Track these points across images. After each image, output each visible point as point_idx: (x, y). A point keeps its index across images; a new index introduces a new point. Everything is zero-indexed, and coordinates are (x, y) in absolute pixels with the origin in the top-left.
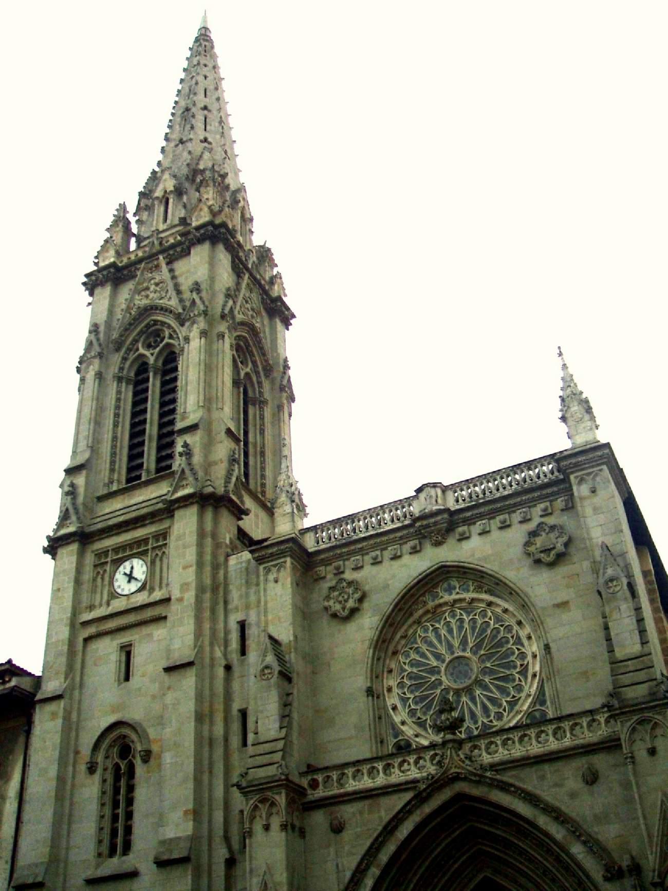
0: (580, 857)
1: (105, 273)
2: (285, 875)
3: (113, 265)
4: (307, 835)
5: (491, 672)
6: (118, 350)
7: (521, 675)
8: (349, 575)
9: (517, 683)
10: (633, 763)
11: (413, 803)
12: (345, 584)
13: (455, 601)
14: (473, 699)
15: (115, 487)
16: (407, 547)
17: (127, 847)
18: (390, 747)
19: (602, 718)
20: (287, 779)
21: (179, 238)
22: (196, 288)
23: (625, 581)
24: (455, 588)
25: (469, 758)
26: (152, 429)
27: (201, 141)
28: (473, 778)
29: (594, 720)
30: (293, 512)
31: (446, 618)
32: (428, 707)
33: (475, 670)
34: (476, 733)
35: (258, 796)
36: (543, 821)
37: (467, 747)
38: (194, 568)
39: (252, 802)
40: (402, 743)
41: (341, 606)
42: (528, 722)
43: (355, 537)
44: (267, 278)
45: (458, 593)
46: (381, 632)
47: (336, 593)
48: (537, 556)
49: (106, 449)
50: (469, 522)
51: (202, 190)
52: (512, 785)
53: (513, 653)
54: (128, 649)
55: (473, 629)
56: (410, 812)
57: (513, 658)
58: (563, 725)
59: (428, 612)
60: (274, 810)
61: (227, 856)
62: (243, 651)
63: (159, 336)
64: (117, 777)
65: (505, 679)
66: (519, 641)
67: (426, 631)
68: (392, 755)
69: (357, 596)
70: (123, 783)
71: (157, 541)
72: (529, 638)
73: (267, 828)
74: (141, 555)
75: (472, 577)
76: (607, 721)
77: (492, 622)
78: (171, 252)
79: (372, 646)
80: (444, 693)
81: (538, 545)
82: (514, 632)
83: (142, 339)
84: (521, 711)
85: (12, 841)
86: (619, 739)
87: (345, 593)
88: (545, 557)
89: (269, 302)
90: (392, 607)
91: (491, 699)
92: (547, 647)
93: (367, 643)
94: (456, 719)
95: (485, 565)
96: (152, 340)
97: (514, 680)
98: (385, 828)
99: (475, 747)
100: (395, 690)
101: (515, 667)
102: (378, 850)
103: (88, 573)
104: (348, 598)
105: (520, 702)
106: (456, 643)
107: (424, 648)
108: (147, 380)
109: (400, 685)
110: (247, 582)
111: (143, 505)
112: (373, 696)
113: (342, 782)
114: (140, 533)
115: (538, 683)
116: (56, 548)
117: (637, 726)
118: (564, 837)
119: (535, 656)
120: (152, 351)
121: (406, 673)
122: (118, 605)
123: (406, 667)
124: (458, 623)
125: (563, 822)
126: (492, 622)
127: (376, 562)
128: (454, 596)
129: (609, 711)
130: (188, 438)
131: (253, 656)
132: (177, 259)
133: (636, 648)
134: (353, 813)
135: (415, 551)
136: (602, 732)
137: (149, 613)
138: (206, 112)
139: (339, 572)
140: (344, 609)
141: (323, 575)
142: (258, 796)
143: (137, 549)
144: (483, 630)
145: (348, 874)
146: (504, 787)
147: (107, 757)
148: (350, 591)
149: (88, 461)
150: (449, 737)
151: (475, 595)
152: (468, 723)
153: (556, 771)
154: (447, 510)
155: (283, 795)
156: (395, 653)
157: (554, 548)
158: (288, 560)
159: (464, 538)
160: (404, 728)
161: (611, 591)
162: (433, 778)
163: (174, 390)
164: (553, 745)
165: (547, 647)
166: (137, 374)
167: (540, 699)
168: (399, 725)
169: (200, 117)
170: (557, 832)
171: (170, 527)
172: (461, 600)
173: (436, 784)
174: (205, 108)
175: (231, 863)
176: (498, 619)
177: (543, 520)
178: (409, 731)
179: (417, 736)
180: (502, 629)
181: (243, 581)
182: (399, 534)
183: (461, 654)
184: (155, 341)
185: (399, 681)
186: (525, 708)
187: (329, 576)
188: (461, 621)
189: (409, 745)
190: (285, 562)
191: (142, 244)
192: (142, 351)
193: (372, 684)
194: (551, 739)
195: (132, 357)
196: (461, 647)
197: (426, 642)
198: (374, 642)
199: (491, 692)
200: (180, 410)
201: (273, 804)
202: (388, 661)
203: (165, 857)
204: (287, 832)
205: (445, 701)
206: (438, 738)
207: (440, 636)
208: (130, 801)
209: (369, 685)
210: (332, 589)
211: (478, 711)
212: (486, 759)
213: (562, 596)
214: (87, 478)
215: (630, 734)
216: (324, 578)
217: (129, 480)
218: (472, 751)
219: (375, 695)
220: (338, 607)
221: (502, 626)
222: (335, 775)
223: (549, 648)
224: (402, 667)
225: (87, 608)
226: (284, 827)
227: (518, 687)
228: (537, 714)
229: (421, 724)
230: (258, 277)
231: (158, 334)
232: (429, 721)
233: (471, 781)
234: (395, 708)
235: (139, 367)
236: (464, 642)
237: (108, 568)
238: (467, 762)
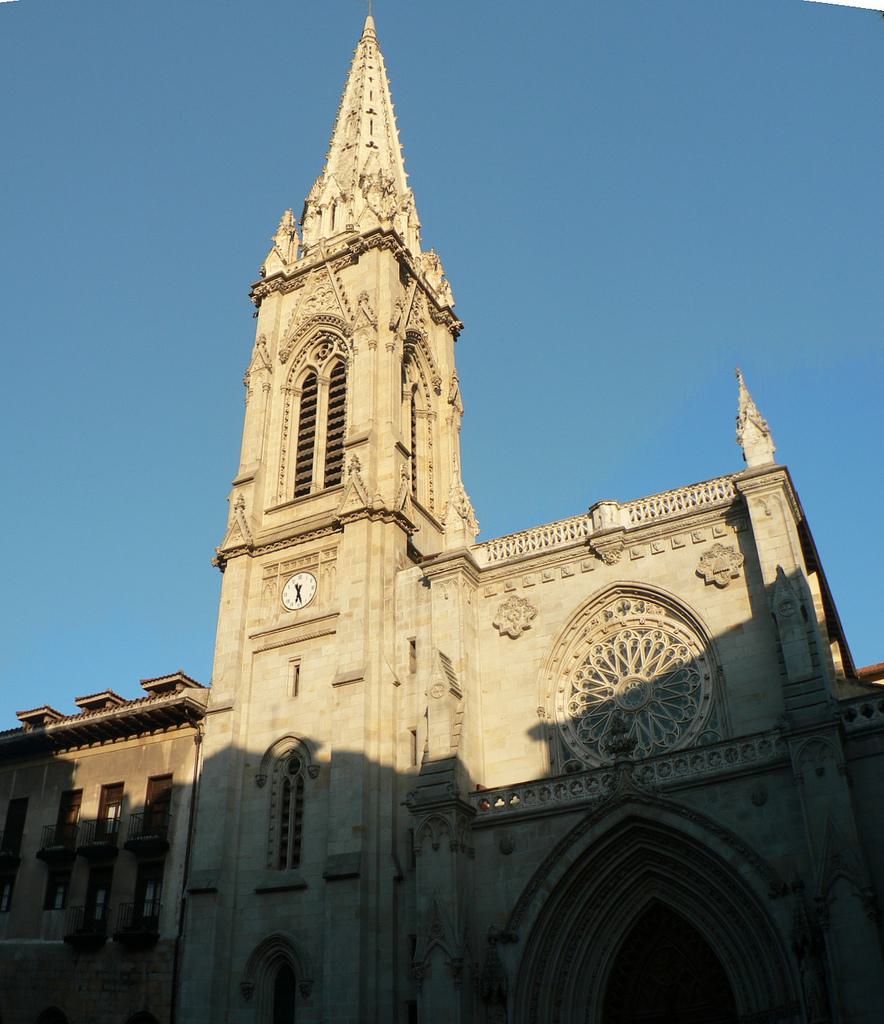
1: (272, 282)
3: (281, 275)
6: (283, 363)
8: (521, 593)
10: (803, 783)
12: (516, 602)
14: (645, 721)
15: (283, 501)
17: (296, 859)
18: (561, 769)
19: (773, 739)
20: (458, 799)
21: (347, 246)
22: (364, 298)
23: (799, 604)
24: (629, 608)
25: (641, 780)
26: (321, 442)
27: (367, 146)
28: (644, 800)
30: (464, 529)
32: (600, 730)
34: (647, 755)
36: (712, 842)
37: (639, 769)
38: (364, 583)
39: (422, 820)
40: (573, 765)
42: (699, 744)
43: (528, 555)
44: (435, 288)
49: (273, 462)
50: (642, 540)
51: (369, 196)
52: (682, 807)
53: (686, 675)
54: (296, 663)
56: (580, 834)
57: (685, 680)
58: (734, 747)
61: (396, 874)
62: (413, 671)
63: (326, 347)
64: (287, 791)
65: (678, 700)
67: (599, 651)
68: (563, 777)
69: (529, 614)
70: (292, 797)
71: (327, 554)
73: (436, 847)
74: (309, 569)
76: (777, 744)
78: (339, 261)
80: (616, 714)
83: (309, 351)
84: (692, 734)
85: (185, 846)
86: (790, 760)
89: (436, 310)
91: (663, 721)
92: (720, 669)
94: (629, 741)
96: (319, 349)
97: (686, 702)
98: (556, 849)
99: (647, 768)
103: (257, 585)
105: (692, 724)
107: (598, 668)
108: (315, 392)
110: (417, 598)
111: (313, 519)
114: (309, 547)
116: (226, 561)
119: (707, 679)
120: (319, 362)
122: (287, 619)
123: (579, 688)
124: (632, 644)
125: (732, 842)
127: (548, 580)
129: (782, 733)
130: (357, 451)
131: (423, 673)
132: (343, 268)
133: (809, 670)
135: (587, 570)
136: (774, 752)
137: (316, 628)
138: (372, 115)
139: (510, 590)
143: (308, 563)
144: (657, 652)
146: (675, 809)
147: (276, 771)
149: (257, 471)
150: (621, 758)
152: (640, 745)
154: (623, 530)
155: (454, 814)
158: (460, 575)
159: (636, 557)
160: (575, 749)
161: (785, 614)
162: (604, 800)
163: (342, 402)
164: (725, 766)
165: (720, 669)
166: (304, 386)
167: (712, 721)
168: (571, 747)
169: (366, 118)
170: (727, 853)
171: (339, 542)
173: (607, 806)
174: (371, 111)
175: (399, 879)
176: (673, 640)
177: (718, 541)
178: (579, 752)
179: (587, 758)
181: (414, 597)
182: (573, 551)
184: (324, 352)
186: (696, 730)
187: (499, 594)
188: (636, 642)
189: (579, 767)
190: (457, 578)
191: (309, 253)
192: (311, 362)
194: (724, 761)
195: (299, 368)
199: (664, 714)
200: (348, 424)
201: (444, 823)
203: (335, 872)
205: (617, 721)
206: (610, 760)
207: (613, 656)
208: (299, 815)
210: (505, 606)
211: (650, 733)
212: (658, 781)
214: (256, 491)
217: (297, 494)
218: (645, 773)
224: (574, 688)
225: (256, 621)
227: (690, 709)
228: (709, 736)
229: (593, 746)
230: (425, 285)
231: (326, 344)
232: (600, 743)
233: (644, 803)
235: (308, 378)
237: (279, 581)
238: (640, 784)
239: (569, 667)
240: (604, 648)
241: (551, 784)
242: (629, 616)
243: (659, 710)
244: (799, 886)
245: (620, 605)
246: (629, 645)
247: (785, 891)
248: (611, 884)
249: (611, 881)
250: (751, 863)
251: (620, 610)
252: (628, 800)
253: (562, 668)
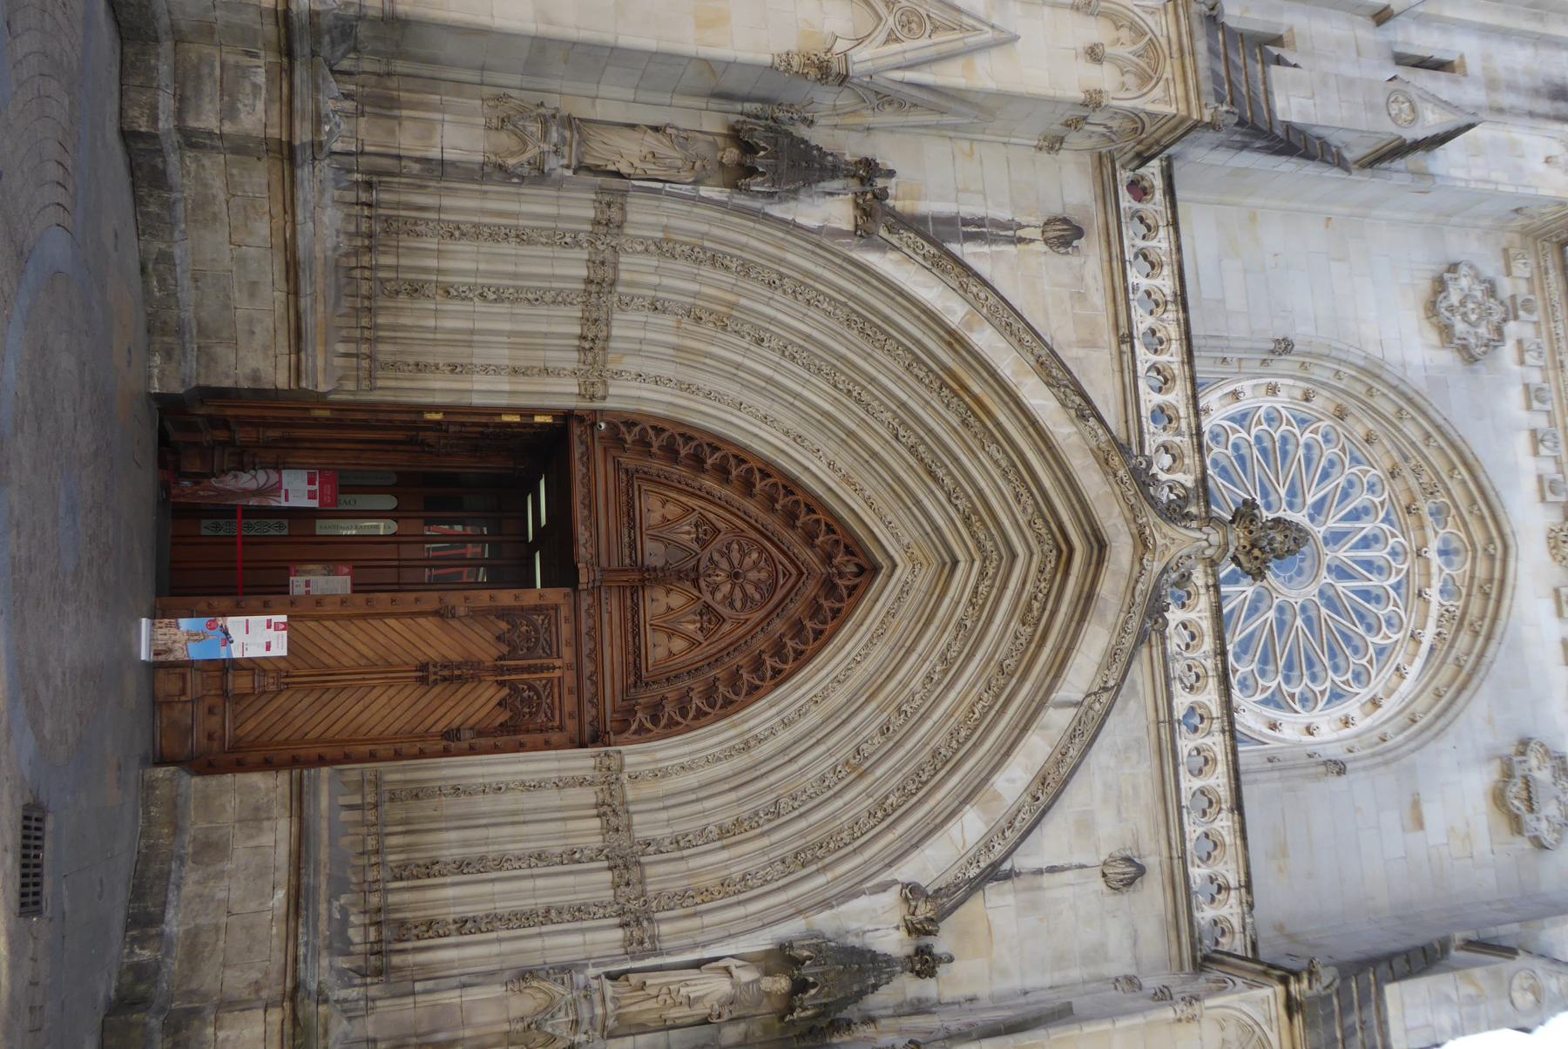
0: (953, 828)
2: (991, 85)
4: (1044, 156)
5: (1281, 623)
7: (1273, 694)
9: (1260, 681)
10: (1180, 1020)
11: (1100, 431)
12: (1496, 318)
13: (1428, 560)
16: (1549, 468)
24: (1449, 564)
28: (1140, 586)
29: (1228, 889)
31: (1394, 535)
33: (1294, 593)
35: (1163, 41)
36: (1037, 748)
41: (1456, 303)
45: (1441, 570)
46: (1394, 388)
47: (1479, 294)
48: (1518, 772)
55: (1366, 594)
59: (1414, 500)
60: (1130, 80)
66: (1336, 696)
67: (1371, 488)
69: (1472, 341)
72: (1347, 722)
73: (1094, 54)
75: (1475, 610)
77: (1377, 640)
79: (1370, 368)
81: (1537, 774)
82: (1355, 689)
87: (1480, 318)
88: (1514, 789)
90: (1440, 421)
93: (1375, 352)
95: (1503, 647)
97: (1263, 673)
100: (1267, 403)
101: (1288, 680)
102: (1006, 330)
104: (1470, 324)
106: (1344, 554)
109: (1276, 414)
112: (1273, 352)
113: (1141, 258)
115: (1261, 733)
117: (1256, 1037)
118: (997, 797)
121: (1297, 431)
123: (1307, 435)
126: (1377, 640)
127: (1532, 395)
128: (1436, 561)
134: (1082, 278)
140: (1451, 309)
141: (1516, 272)
142: (1163, 41)
145: (954, 247)
146: (1120, 660)
148: (1482, 330)
151: (1434, 611)
153: (1135, 788)
156: (1341, 414)
157: (1531, 810)
170: (1013, 780)
172: (1428, 575)
180: (1364, 662)
183: (1326, 560)
185: (1284, 412)
193: (1298, 354)
196: (1337, 562)
197: (1351, 484)
198: (1377, 371)
201: (1145, 78)
202: (1328, 394)
204: (1084, 105)
207: (1358, 519)
209: (1296, 348)
210: (1492, 291)
213: (1433, 814)
215: (1238, 1020)
216: (1509, 274)
219: (1272, 357)
220: (1455, 299)
221: (1370, 662)
222: (1161, 243)
223: (1339, 773)
226: (1093, 101)
234: (1235, 395)
236: (1341, 573)
239: (1349, 420)
240: (1377, 500)
241: (1177, 359)
242: (1436, 561)
243: (1254, 609)
244: (925, 963)
245: (1455, 544)
246: (1376, 554)
247: (914, 930)
248: (940, 473)
249: (950, 473)
250: (989, 848)
251: (1445, 541)
252: (1143, 542)
253: (1352, 406)
